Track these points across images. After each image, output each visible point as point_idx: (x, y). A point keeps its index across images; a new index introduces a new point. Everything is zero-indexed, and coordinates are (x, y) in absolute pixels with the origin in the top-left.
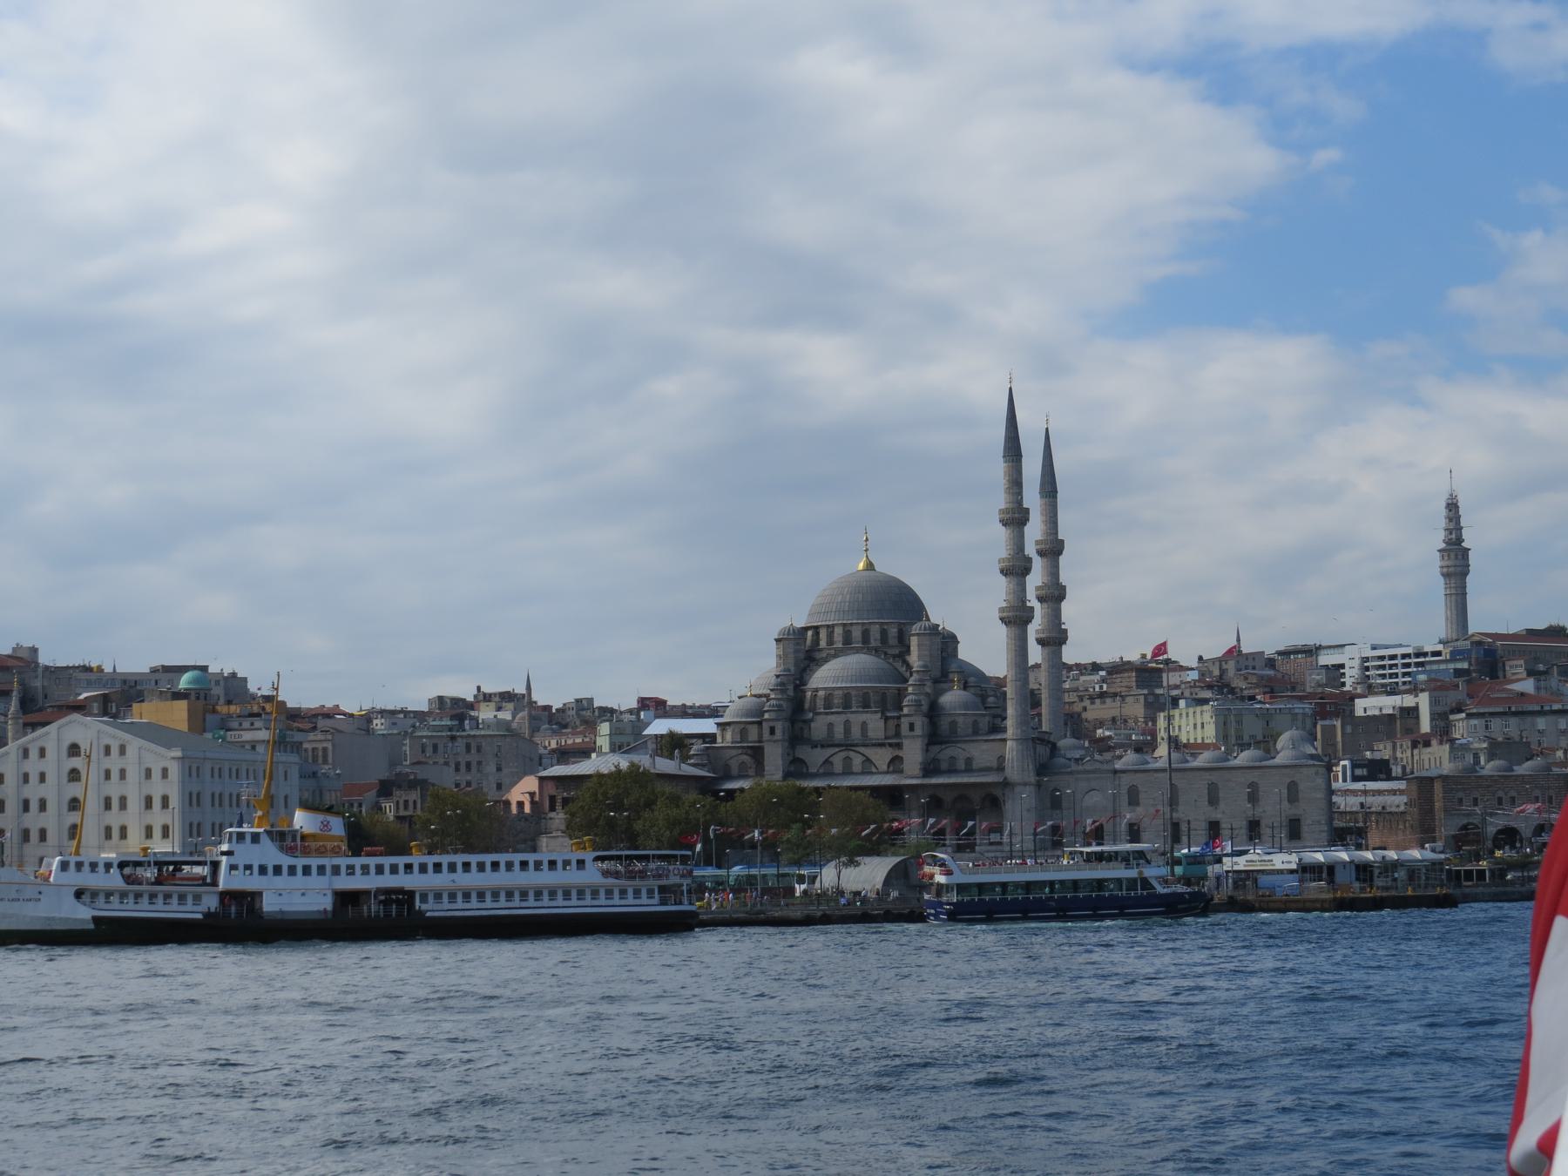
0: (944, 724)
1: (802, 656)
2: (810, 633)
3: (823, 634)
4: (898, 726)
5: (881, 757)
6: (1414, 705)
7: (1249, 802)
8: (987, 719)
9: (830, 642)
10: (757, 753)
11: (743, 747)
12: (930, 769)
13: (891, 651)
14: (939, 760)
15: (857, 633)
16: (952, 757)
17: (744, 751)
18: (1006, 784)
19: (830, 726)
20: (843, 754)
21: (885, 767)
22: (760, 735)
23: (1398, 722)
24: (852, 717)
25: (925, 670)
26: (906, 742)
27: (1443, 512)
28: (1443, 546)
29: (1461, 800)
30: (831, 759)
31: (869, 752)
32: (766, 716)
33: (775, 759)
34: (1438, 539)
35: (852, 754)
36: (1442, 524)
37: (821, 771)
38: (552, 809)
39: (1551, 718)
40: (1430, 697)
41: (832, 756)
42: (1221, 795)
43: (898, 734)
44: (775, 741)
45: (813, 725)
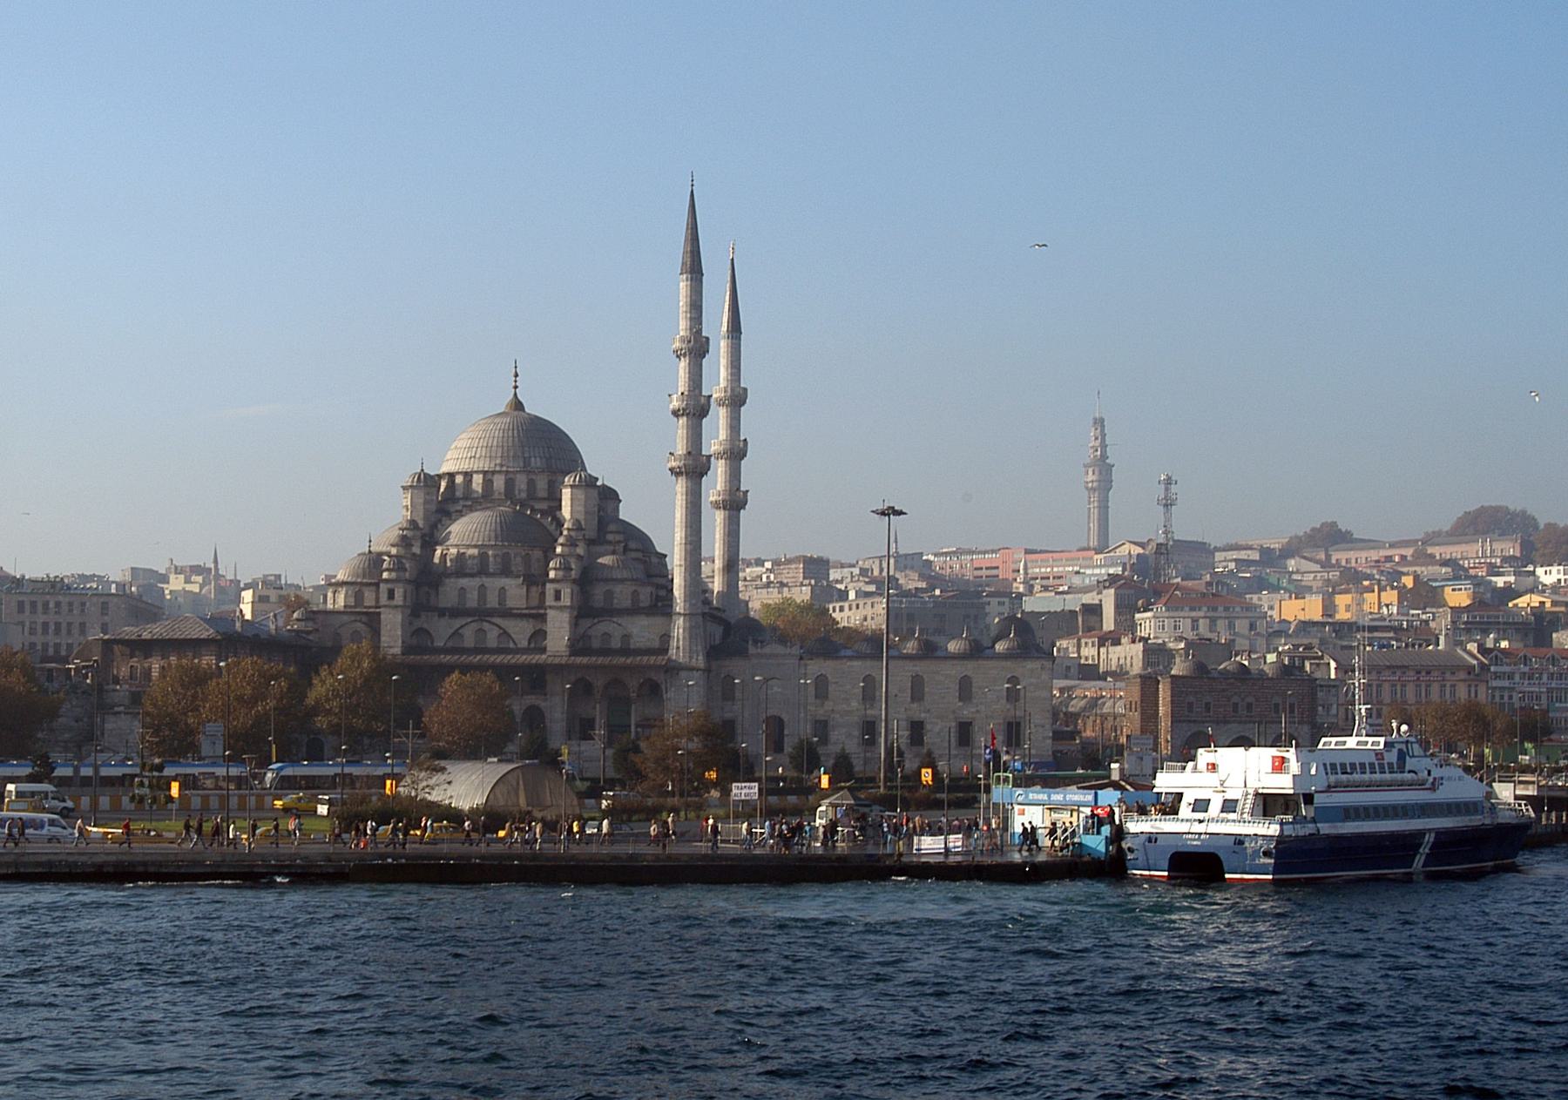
1: (433, 507)
4: (543, 594)
5: (520, 631)
6: (1097, 602)
7: (960, 700)
11: (359, 613)
12: (579, 645)
14: (590, 637)
16: (605, 634)
17: (358, 618)
18: (673, 669)
20: (475, 626)
21: (524, 644)
22: (377, 599)
23: (1080, 619)
24: (487, 581)
25: (578, 526)
26: (551, 613)
29: (1190, 705)
32: (385, 575)
35: (485, 624)
37: (450, 644)
40: (1116, 595)
41: (462, 627)
42: (926, 689)
43: (542, 604)
44: (396, 607)
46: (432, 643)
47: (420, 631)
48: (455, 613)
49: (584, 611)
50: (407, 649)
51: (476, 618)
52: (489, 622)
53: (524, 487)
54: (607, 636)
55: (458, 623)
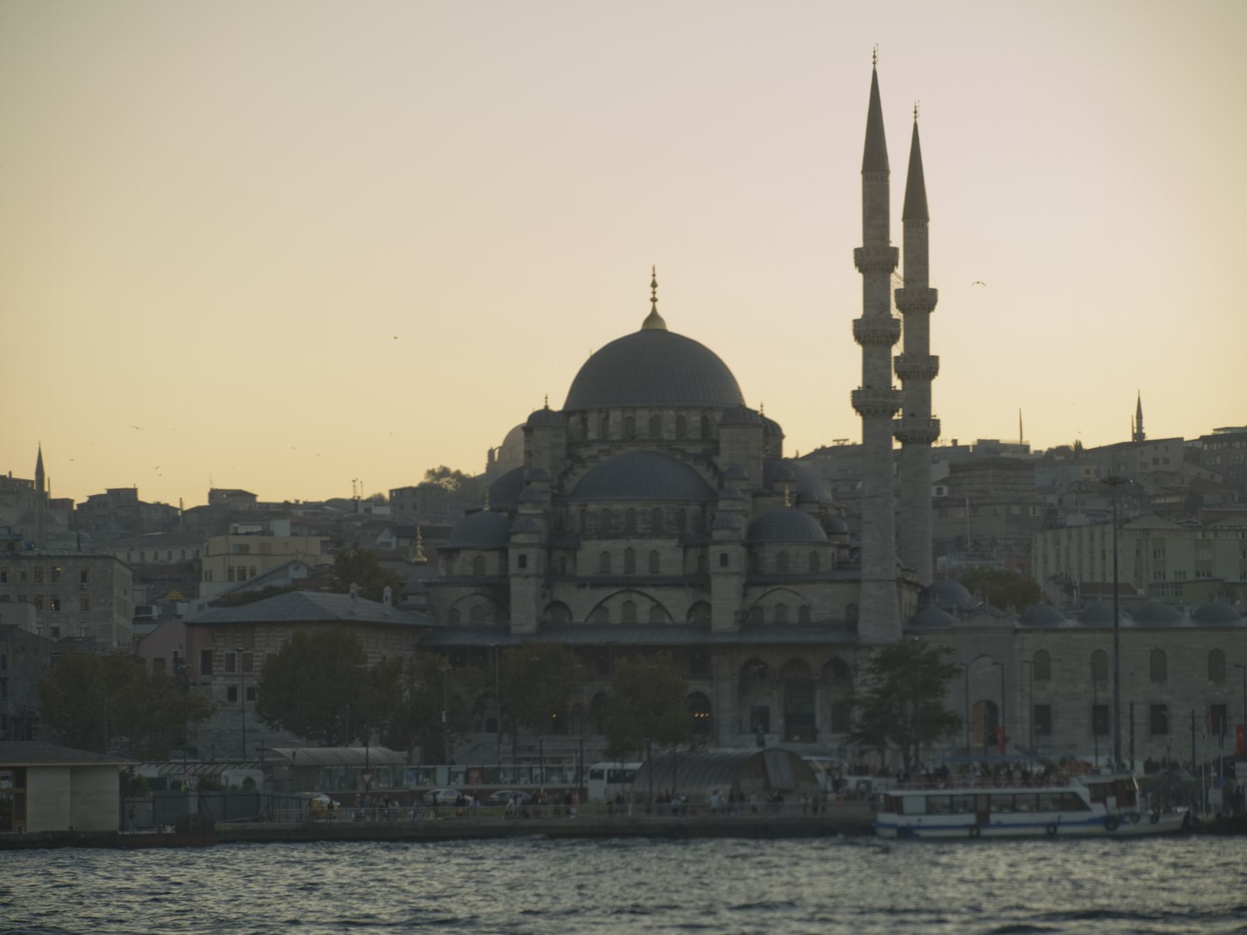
4: (703, 559)
5: (678, 603)
8: (830, 550)
12: (749, 619)
13: (691, 449)
19: (606, 555)
21: (681, 618)
22: (505, 566)
24: (635, 543)
26: (716, 582)
30: (605, 604)
31: (660, 594)
35: (635, 597)
37: (591, 621)
38: (207, 668)
41: (607, 599)
45: (579, 554)
46: (571, 618)
47: (555, 605)
48: (597, 583)
49: (755, 578)
50: (543, 627)
51: (624, 588)
52: (637, 592)
53: (672, 426)
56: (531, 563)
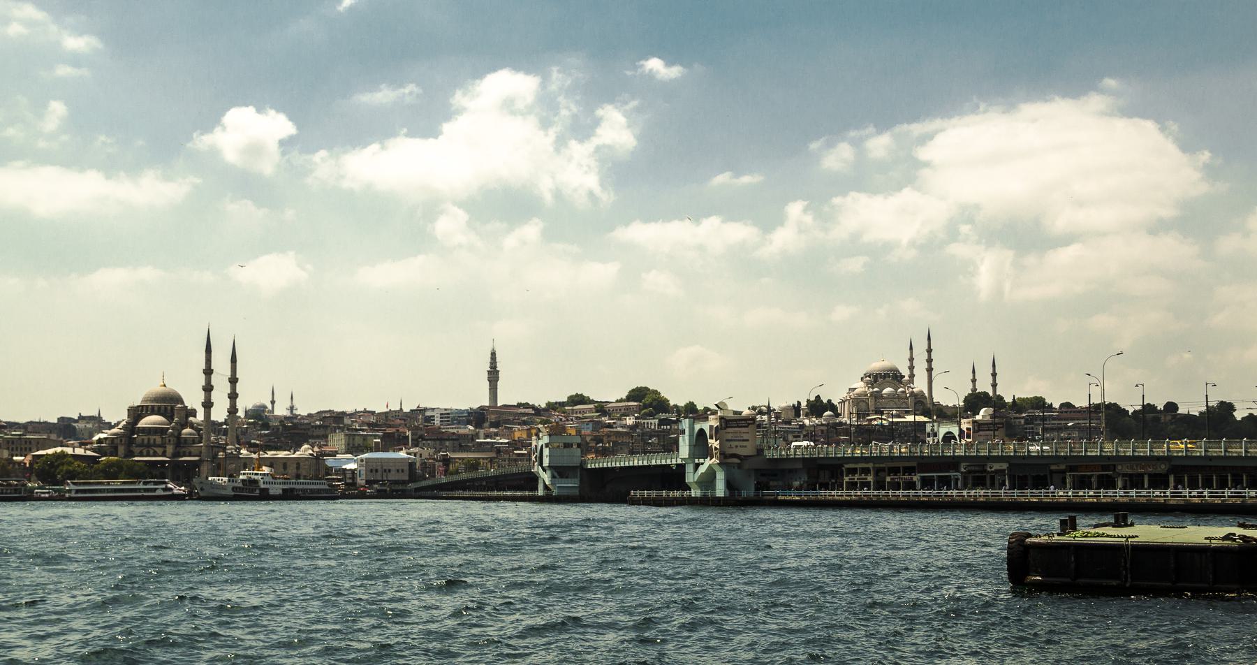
0: (182, 441)
2: (140, 408)
3: (144, 408)
5: (159, 450)
9: (147, 411)
10: (116, 448)
15: (156, 409)
19: (143, 439)
26: (168, 446)
27: (490, 356)
28: (489, 369)
31: (155, 449)
33: (121, 450)
34: (487, 367)
36: (489, 360)
39: (451, 442)
54: (184, 452)
55: (142, 448)
56: (123, 442)
